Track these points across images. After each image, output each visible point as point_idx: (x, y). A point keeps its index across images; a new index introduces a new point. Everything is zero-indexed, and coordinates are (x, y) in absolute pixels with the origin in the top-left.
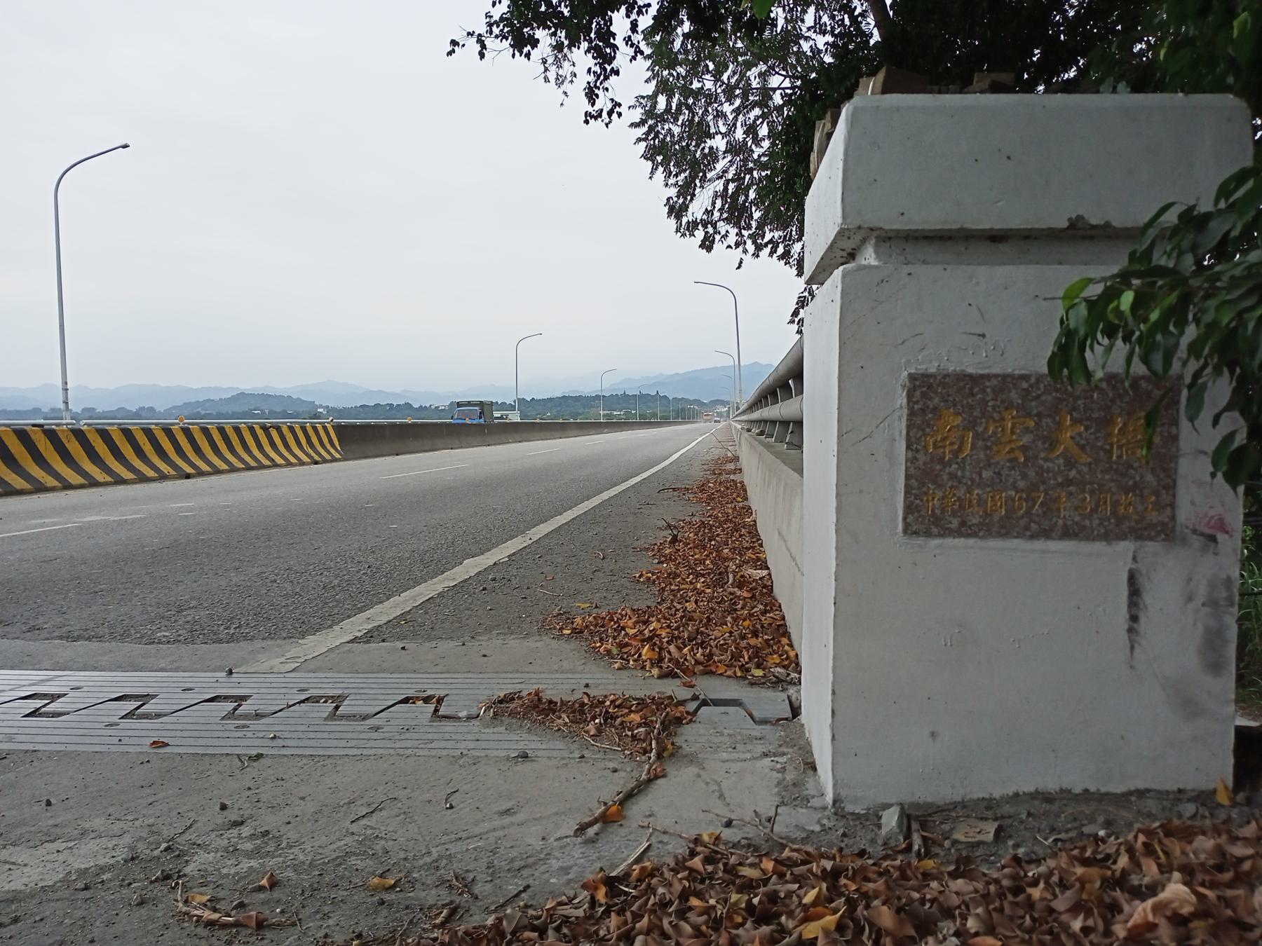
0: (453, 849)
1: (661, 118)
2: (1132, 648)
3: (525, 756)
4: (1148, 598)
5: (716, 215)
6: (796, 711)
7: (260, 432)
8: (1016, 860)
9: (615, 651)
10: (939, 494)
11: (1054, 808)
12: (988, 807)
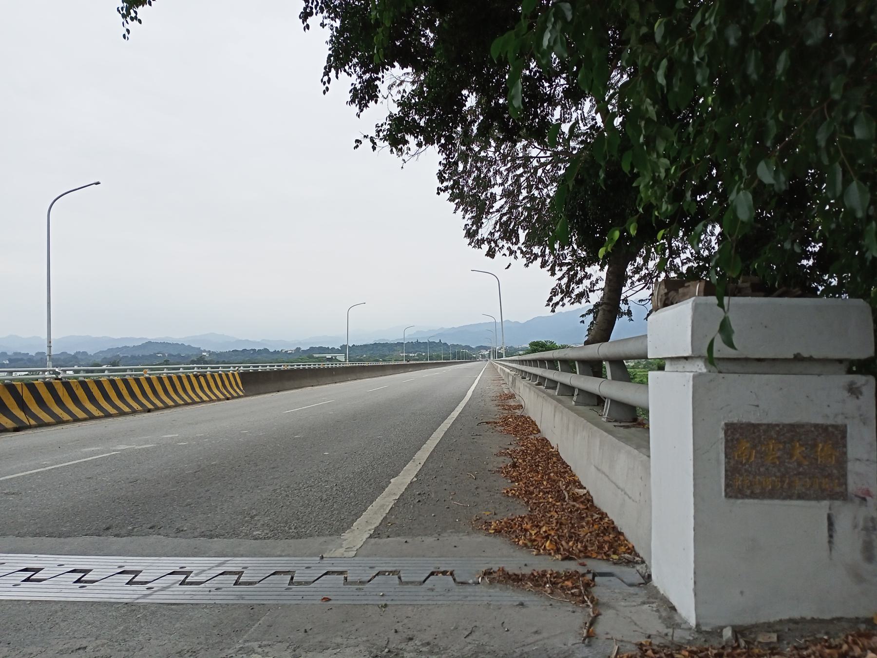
0: (526, 649)
1: (461, 175)
2: (831, 550)
4: (837, 527)
5: (497, 235)
7: (193, 379)
8: (796, 648)
9: (529, 544)
10: (741, 478)
11: (800, 626)
12: (769, 627)
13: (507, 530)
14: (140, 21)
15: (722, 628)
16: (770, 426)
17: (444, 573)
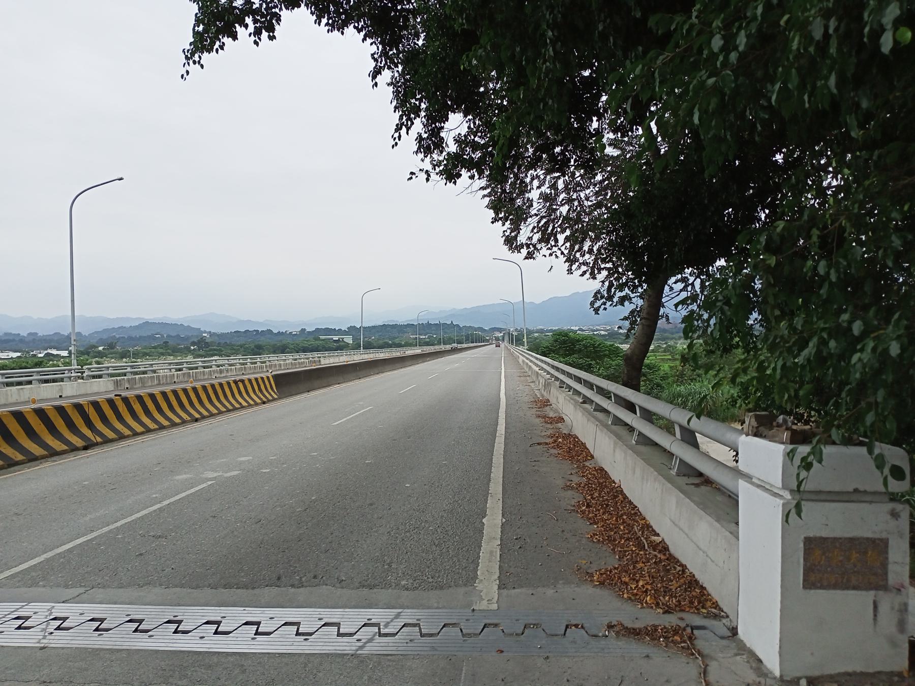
3: (648, 656)
6: (734, 631)
9: (633, 598)
13: (607, 580)
14: (202, 66)
15: (799, 679)
16: (835, 539)
17: (576, 626)
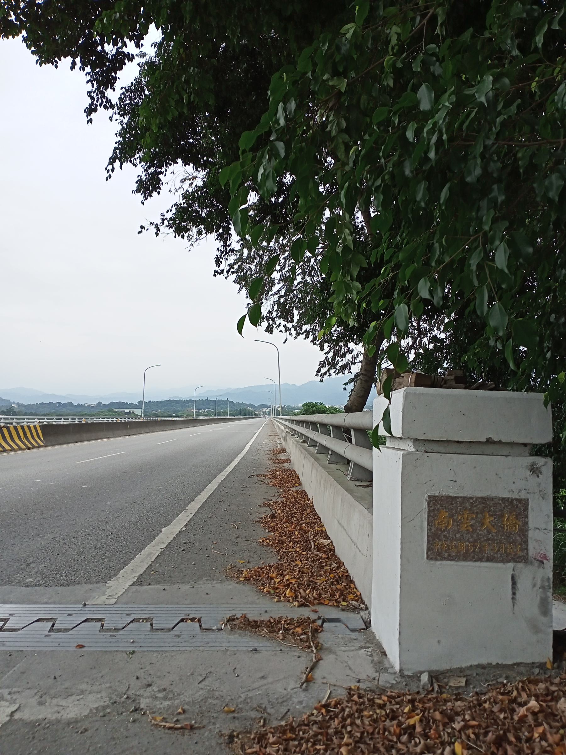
0: (250, 694)
1: (245, 261)
2: (514, 605)
3: (255, 650)
4: (519, 586)
5: (274, 314)
6: (368, 624)
8: (477, 693)
9: (272, 592)
10: (440, 543)
11: (486, 671)
12: (460, 672)
13: (255, 578)
15: (422, 673)
17: (192, 620)
